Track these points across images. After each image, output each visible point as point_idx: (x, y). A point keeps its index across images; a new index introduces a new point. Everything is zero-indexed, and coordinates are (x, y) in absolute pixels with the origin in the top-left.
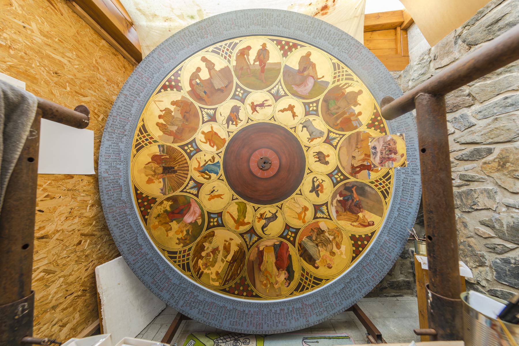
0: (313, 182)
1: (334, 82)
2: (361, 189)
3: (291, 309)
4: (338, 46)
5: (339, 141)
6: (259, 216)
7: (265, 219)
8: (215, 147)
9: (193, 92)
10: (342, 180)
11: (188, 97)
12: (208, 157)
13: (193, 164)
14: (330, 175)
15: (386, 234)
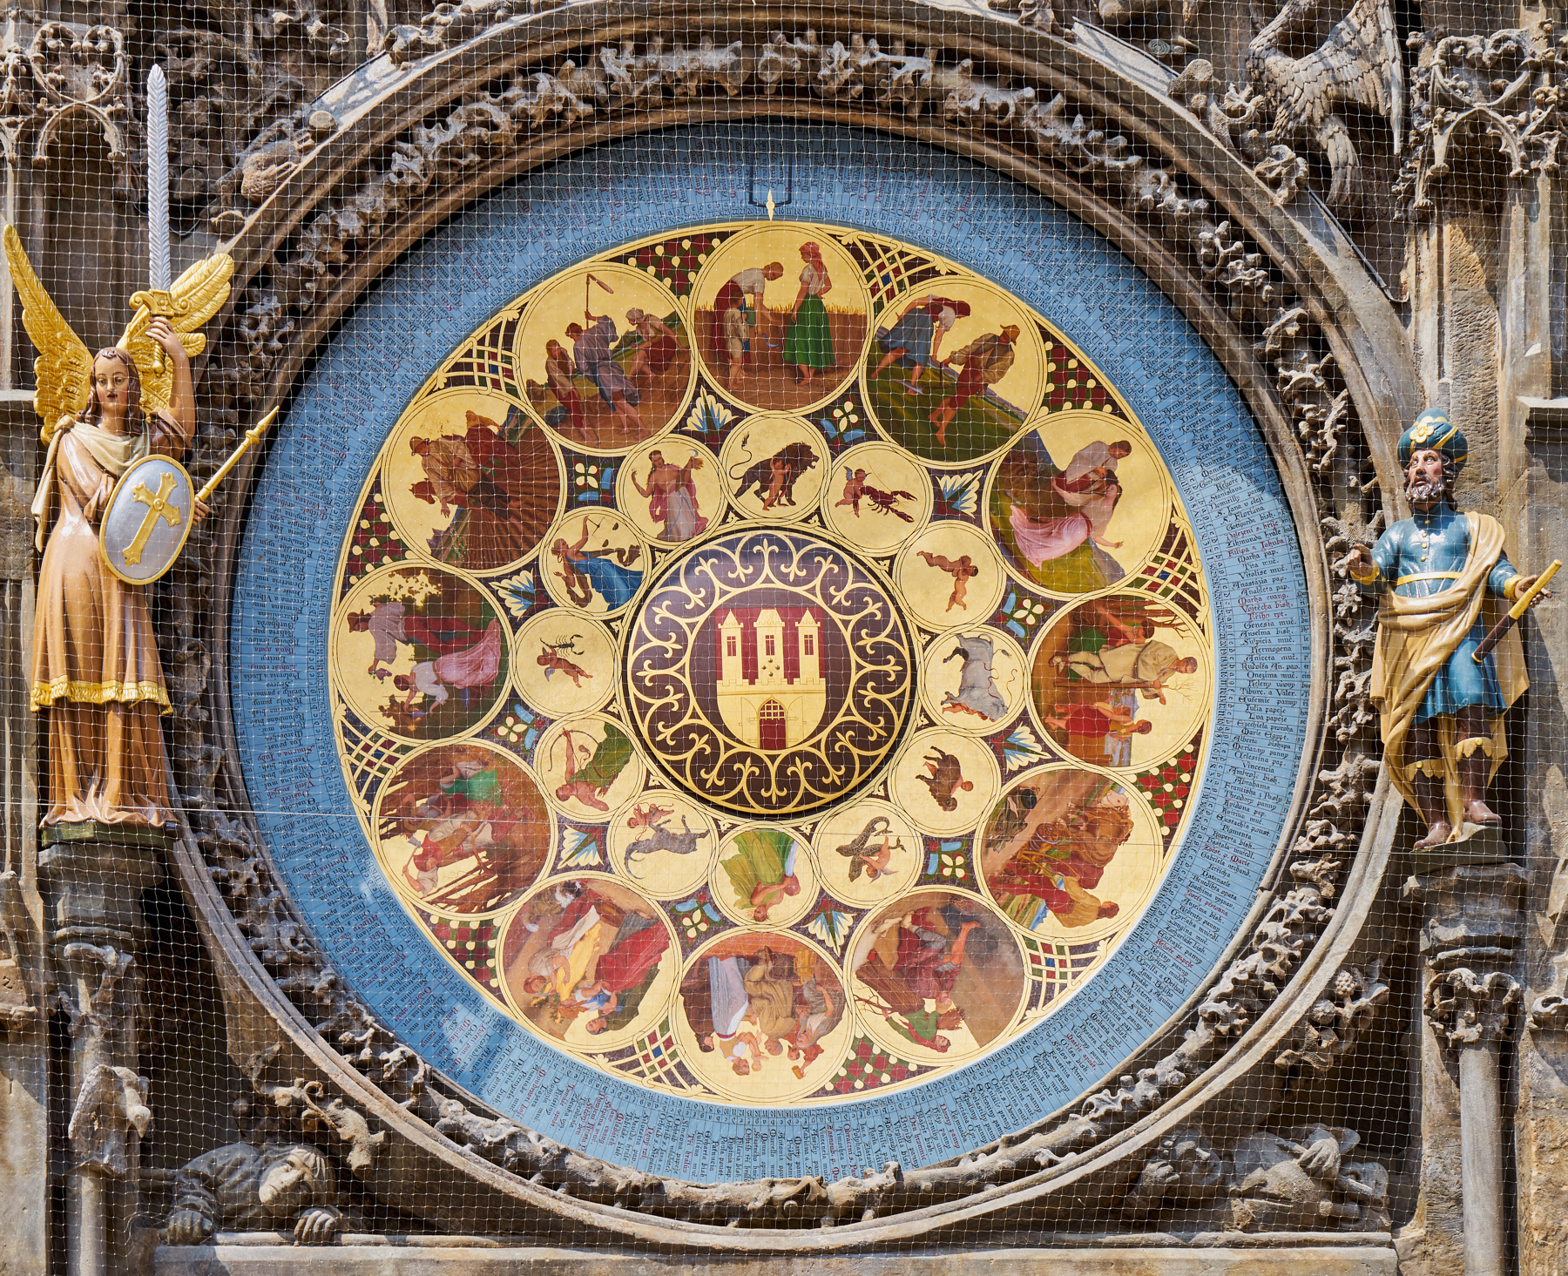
0: (870, 828)
1: (1138, 583)
2: (989, 941)
3: (562, 1086)
4: (1219, 487)
5: (1031, 765)
6: (645, 810)
7: (659, 830)
8: (661, 526)
9: (713, 325)
10: (953, 880)
11: (689, 326)
12: (623, 541)
13: (567, 527)
14: (932, 845)
15: (957, 1094)
